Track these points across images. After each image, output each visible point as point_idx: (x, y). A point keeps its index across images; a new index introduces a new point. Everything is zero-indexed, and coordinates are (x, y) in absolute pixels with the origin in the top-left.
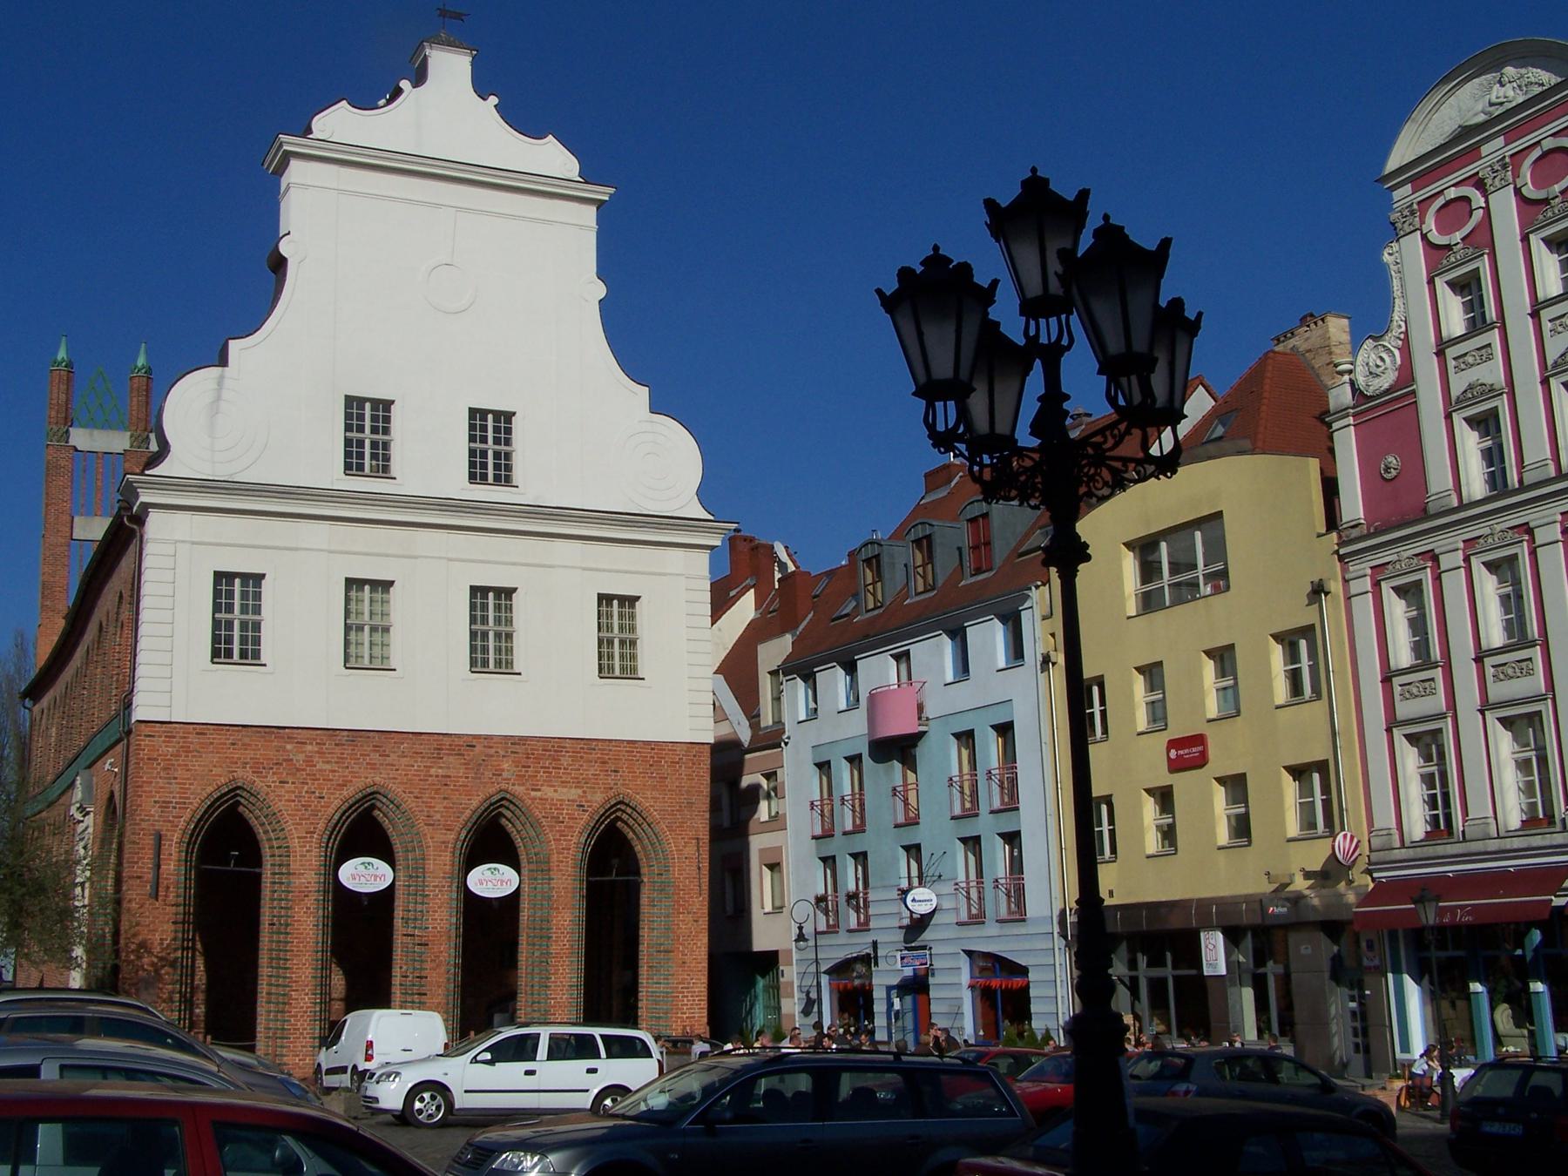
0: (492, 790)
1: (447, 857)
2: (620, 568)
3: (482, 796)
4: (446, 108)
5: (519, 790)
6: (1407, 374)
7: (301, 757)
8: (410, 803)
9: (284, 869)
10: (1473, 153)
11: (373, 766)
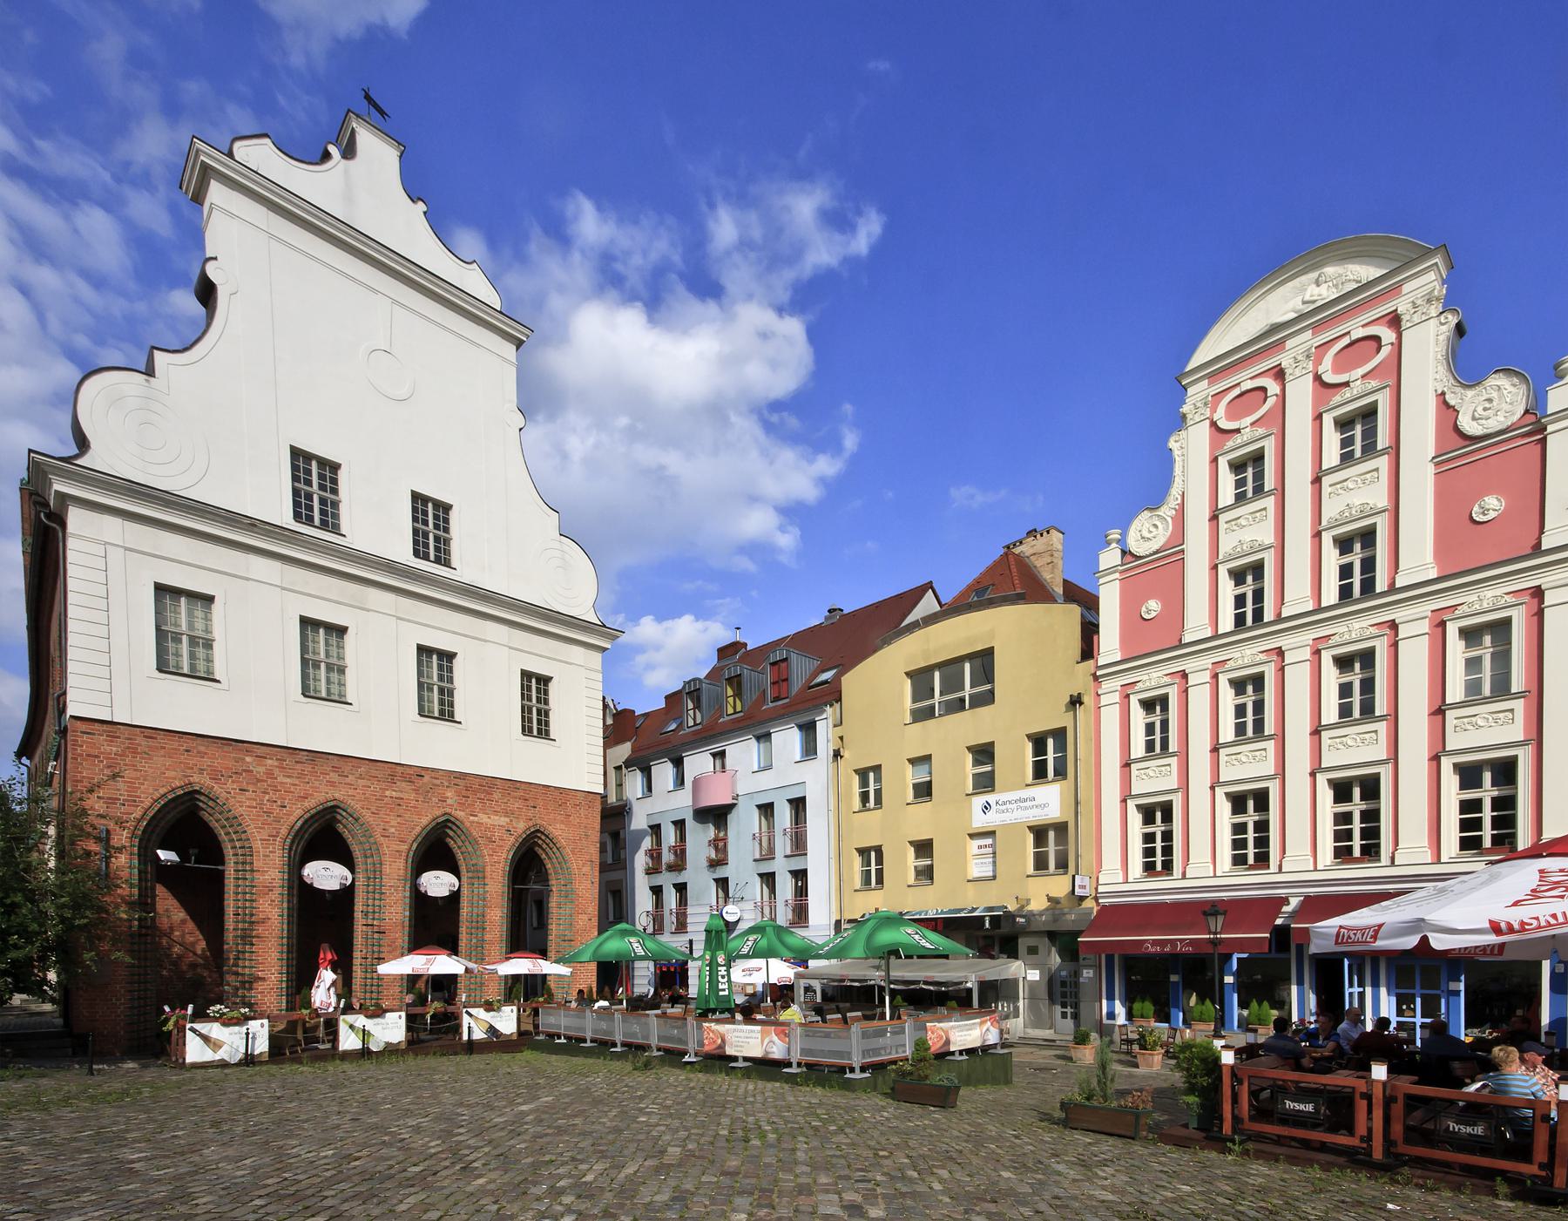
0: (438, 813)
3: (430, 817)
5: (460, 814)
7: (262, 769)
8: (367, 816)
9: (246, 865)
11: (332, 784)
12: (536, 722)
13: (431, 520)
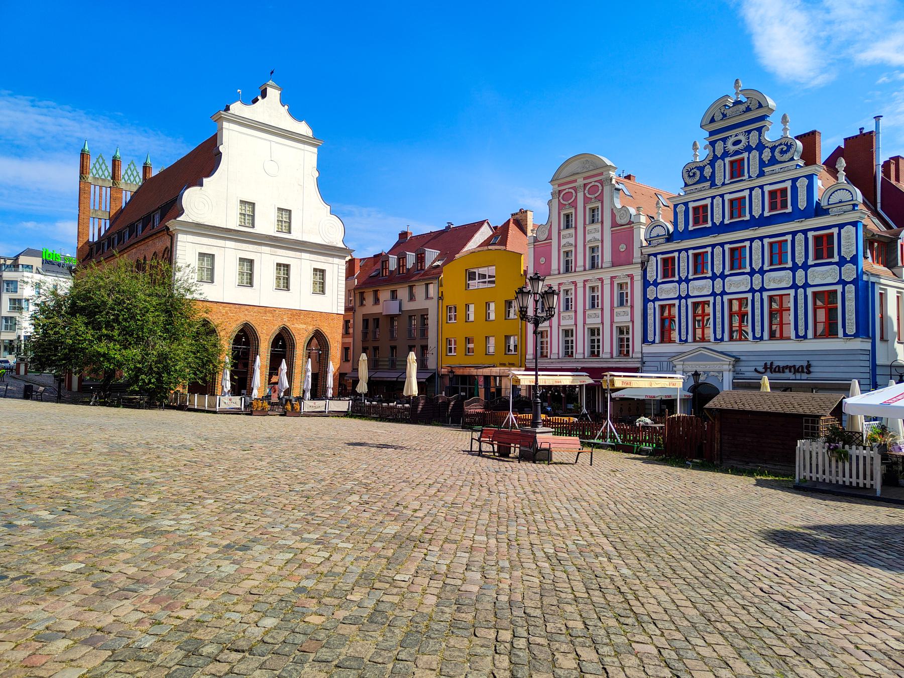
1: (266, 343)
2: (321, 262)
4: (271, 108)
5: (288, 324)
6: (549, 237)
10: (575, 181)
11: (245, 315)
12: (320, 287)
13: (285, 215)
